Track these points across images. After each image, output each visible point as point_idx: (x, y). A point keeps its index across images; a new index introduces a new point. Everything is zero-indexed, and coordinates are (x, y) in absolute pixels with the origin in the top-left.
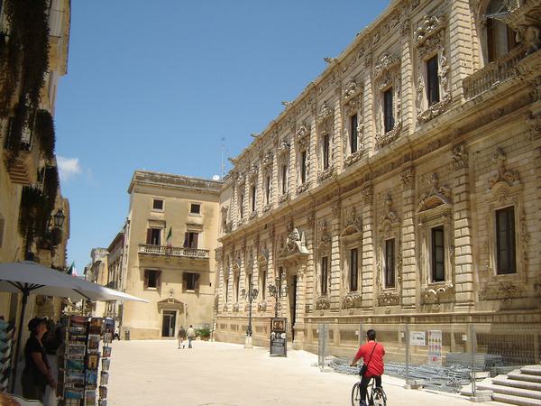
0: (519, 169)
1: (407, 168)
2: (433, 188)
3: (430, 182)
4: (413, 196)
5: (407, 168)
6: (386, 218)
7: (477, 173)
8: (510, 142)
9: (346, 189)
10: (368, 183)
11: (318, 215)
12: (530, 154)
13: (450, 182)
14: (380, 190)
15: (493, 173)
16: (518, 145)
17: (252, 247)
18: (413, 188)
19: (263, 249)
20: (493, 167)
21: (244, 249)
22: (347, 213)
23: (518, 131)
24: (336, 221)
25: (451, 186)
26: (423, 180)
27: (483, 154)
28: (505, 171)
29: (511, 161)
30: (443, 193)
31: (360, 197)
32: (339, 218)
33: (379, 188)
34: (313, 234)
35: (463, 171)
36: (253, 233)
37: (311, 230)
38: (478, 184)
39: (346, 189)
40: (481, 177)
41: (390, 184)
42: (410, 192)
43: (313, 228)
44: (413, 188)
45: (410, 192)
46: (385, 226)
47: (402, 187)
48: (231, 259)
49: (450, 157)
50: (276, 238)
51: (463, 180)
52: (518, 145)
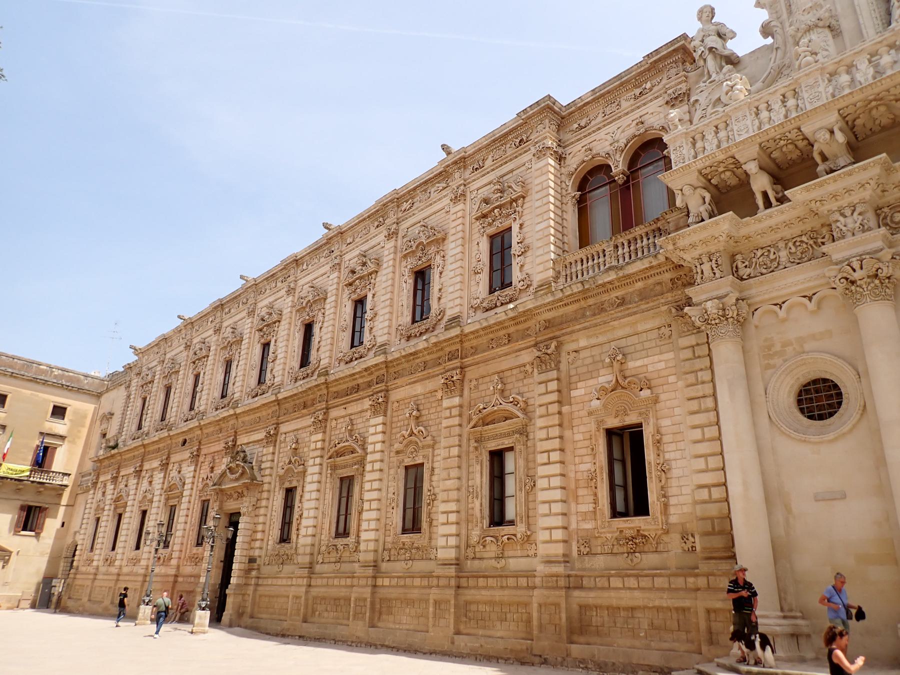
0: (649, 376)
1: (454, 369)
2: (497, 396)
3: (489, 387)
4: (461, 406)
5: (454, 369)
6: (412, 434)
7: (574, 379)
8: (631, 341)
9: (337, 395)
10: (382, 386)
11: (283, 428)
12: (671, 355)
13: (526, 389)
14: (398, 397)
15: (602, 380)
16: (647, 345)
17: (153, 470)
18: (461, 396)
19: (174, 473)
20: (602, 372)
21: (138, 473)
22: (338, 429)
23: (649, 326)
24: (320, 436)
25: (527, 395)
26: (476, 387)
27: (583, 354)
28: (625, 378)
29: (631, 364)
30: (515, 403)
31: (367, 403)
32: (324, 432)
33: (395, 396)
34: (273, 453)
35: (554, 374)
36: (159, 450)
37: (271, 449)
38: (574, 393)
39: (337, 395)
40: (580, 385)
41: (419, 389)
42: (456, 401)
43: (275, 446)
44: (461, 396)
45: (456, 401)
46: (407, 446)
47: (439, 394)
48: (110, 487)
49: (527, 357)
50: (201, 459)
51: (553, 386)
52: (647, 345)
